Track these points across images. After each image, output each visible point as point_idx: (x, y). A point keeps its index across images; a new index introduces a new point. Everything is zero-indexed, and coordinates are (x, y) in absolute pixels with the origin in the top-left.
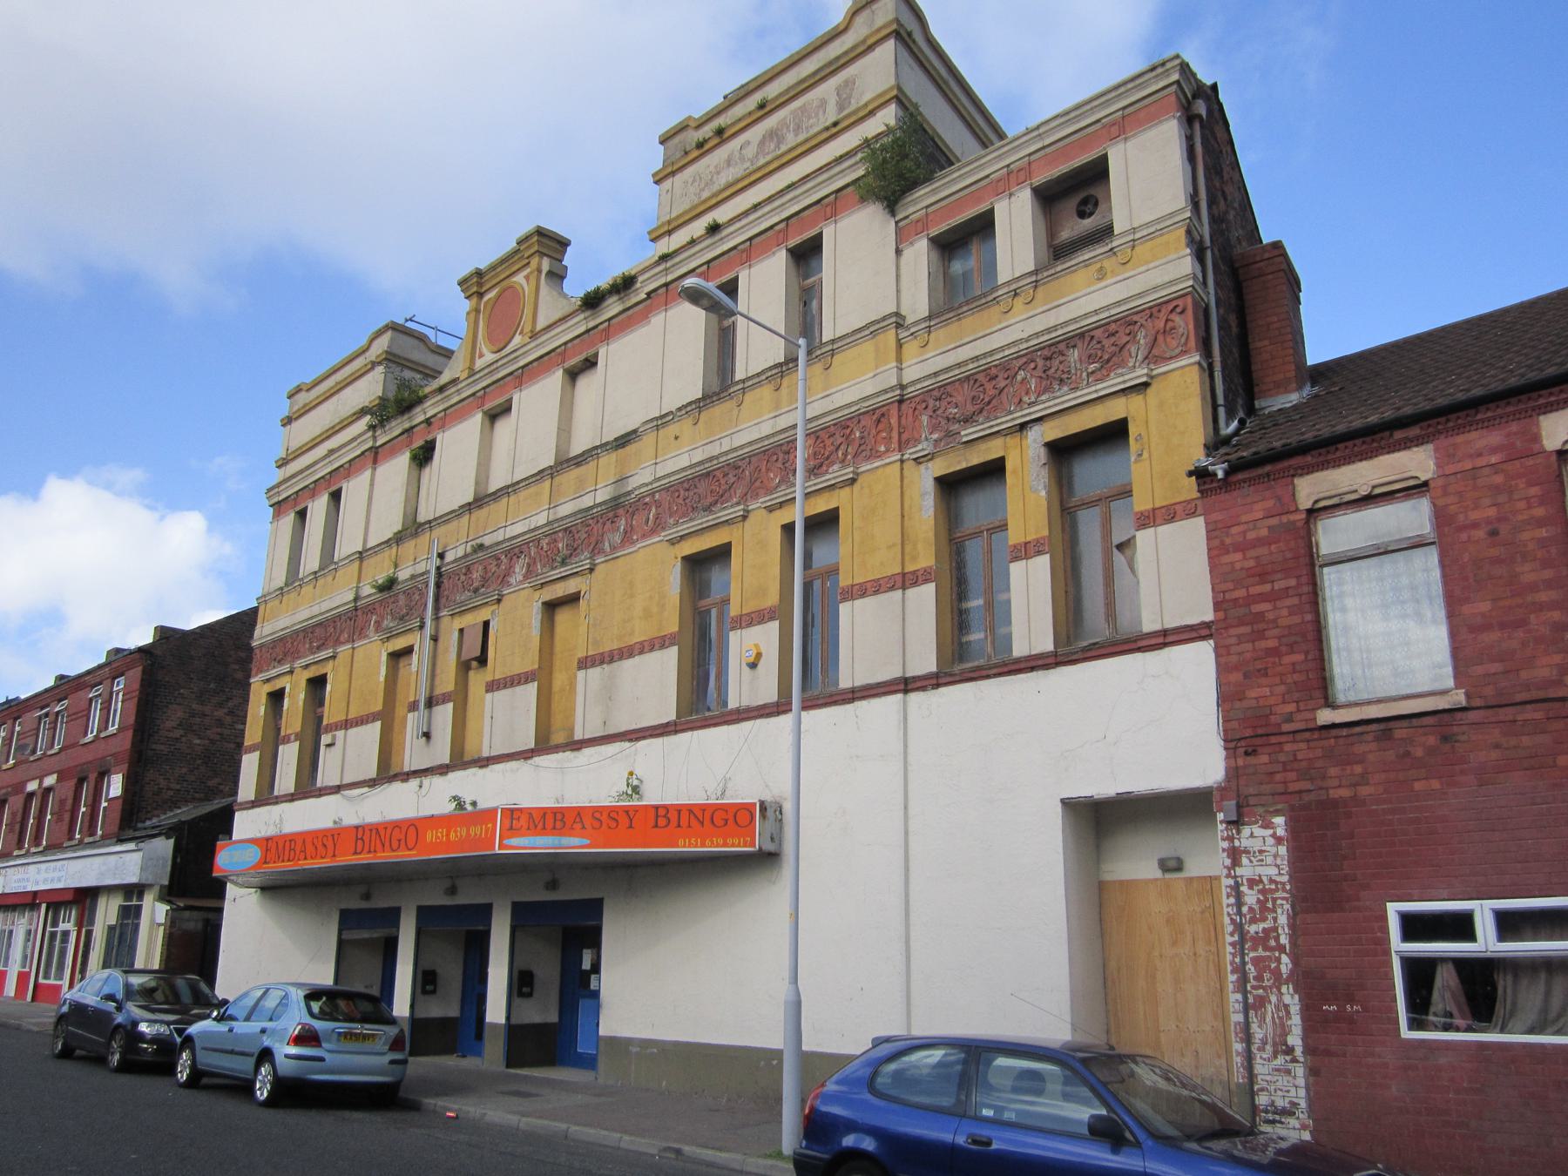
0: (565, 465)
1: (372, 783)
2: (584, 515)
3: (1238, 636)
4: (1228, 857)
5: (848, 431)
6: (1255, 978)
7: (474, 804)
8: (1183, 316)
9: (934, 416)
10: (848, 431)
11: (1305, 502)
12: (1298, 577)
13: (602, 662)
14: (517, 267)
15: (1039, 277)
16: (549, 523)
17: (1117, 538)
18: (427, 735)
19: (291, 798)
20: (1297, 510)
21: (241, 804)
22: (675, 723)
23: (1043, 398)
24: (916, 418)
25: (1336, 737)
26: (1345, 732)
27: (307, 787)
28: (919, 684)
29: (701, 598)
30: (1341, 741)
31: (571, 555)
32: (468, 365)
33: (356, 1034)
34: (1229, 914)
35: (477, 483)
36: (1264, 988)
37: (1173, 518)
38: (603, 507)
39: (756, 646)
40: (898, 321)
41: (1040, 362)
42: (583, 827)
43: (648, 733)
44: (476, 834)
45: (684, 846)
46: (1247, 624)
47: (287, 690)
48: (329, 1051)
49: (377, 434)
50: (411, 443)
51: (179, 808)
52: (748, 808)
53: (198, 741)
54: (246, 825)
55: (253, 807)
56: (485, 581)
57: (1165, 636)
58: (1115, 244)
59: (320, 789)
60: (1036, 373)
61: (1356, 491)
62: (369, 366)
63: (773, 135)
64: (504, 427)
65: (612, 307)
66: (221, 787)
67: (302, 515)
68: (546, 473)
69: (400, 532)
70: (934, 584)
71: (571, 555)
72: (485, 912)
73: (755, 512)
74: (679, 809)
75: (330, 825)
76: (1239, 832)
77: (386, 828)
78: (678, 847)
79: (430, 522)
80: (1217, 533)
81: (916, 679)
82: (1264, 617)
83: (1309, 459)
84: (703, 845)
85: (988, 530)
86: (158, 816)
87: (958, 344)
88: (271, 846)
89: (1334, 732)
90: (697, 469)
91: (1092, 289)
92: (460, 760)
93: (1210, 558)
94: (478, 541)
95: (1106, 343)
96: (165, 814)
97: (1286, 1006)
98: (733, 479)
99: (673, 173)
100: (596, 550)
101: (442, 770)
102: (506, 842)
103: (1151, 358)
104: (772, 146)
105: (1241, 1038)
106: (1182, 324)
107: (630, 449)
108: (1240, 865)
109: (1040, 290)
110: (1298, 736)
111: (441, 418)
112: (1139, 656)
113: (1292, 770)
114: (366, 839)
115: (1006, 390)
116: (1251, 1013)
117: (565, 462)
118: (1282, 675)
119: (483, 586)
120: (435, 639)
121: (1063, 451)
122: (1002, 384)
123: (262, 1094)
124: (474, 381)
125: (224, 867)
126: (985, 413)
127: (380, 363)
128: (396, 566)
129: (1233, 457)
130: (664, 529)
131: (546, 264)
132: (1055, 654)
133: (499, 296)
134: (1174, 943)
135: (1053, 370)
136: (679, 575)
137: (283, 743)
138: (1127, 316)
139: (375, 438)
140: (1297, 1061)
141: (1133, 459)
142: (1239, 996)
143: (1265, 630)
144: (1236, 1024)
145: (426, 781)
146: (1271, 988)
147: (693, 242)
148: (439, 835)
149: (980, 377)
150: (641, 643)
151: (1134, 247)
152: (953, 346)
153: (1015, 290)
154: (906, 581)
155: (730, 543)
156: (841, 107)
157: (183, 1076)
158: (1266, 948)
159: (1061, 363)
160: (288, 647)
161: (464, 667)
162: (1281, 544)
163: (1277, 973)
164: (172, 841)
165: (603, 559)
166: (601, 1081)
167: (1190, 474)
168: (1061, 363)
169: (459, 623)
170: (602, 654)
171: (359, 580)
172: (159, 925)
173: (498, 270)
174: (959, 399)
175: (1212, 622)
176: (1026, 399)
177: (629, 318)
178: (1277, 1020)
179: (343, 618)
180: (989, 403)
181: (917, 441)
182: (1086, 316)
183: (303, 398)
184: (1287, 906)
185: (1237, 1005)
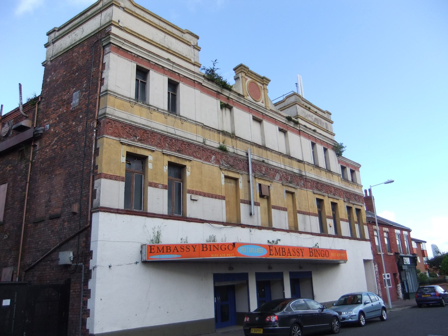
79: (240, 138)
147: (310, 129)
173: (253, 75)
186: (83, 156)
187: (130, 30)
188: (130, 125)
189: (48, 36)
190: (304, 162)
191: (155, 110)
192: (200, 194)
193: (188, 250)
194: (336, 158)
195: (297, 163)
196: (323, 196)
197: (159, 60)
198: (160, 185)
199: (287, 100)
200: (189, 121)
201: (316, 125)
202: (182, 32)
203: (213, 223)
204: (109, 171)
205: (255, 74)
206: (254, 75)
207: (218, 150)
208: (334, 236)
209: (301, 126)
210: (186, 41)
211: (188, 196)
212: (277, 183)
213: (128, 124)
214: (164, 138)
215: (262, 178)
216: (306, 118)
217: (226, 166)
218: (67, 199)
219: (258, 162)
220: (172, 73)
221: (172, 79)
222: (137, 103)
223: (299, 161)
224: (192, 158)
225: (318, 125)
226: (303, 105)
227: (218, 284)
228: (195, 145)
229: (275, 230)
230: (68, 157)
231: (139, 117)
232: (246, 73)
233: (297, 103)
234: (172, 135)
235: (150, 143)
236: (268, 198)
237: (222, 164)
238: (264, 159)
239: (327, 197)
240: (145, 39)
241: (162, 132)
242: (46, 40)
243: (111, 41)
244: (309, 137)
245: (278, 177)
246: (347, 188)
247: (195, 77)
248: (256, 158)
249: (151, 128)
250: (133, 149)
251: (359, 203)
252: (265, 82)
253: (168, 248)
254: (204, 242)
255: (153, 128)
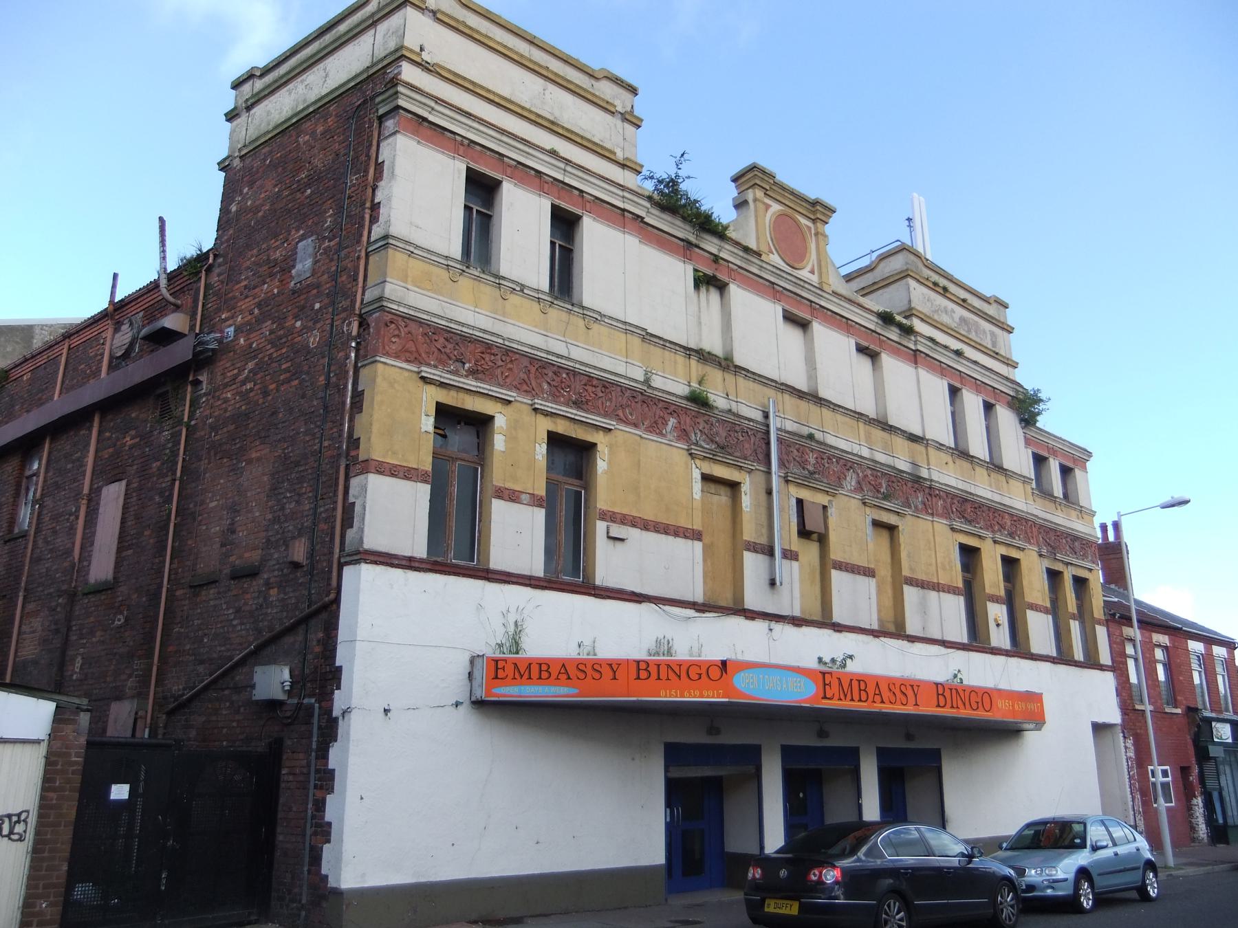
79: (748, 371)
147: (946, 347)
173: (786, 194)
186: (322, 411)
187: (450, 71)
188: (448, 331)
189: (234, 92)
190: (927, 440)
191: (514, 289)
192: (635, 522)
193: (597, 675)
194: (1020, 432)
195: (907, 443)
196: (980, 537)
197: (528, 153)
198: (523, 497)
199: (882, 264)
200: (606, 320)
201: (964, 336)
202: (591, 76)
203: (667, 603)
204: (390, 453)
205: (793, 193)
206: (789, 196)
207: (685, 402)
208: (1007, 653)
209: (919, 338)
210: (603, 100)
211: (601, 526)
212: (847, 498)
213: (442, 329)
214: (537, 366)
215: (806, 483)
216: (936, 317)
217: (706, 449)
218: (276, 527)
219: (797, 438)
220: (562, 188)
221: (563, 205)
222: (467, 270)
223: (913, 438)
224: (612, 423)
225: (970, 336)
227: (677, 773)
228: (623, 389)
229: (838, 628)
230: (281, 415)
231: (473, 309)
232: (767, 190)
233: (911, 274)
234: (559, 360)
235: (500, 379)
236: (822, 539)
237: (695, 441)
238: (813, 431)
239: (989, 542)
240: (491, 97)
241: (532, 352)
242: (229, 100)
243: (401, 102)
244: (941, 369)
245: (851, 481)
246: (1048, 517)
247: (625, 200)
248: (790, 426)
249: (503, 339)
250: (453, 397)
251: (1083, 560)
252: (819, 216)
253: (544, 667)
254: (642, 656)
255: (510, 340)
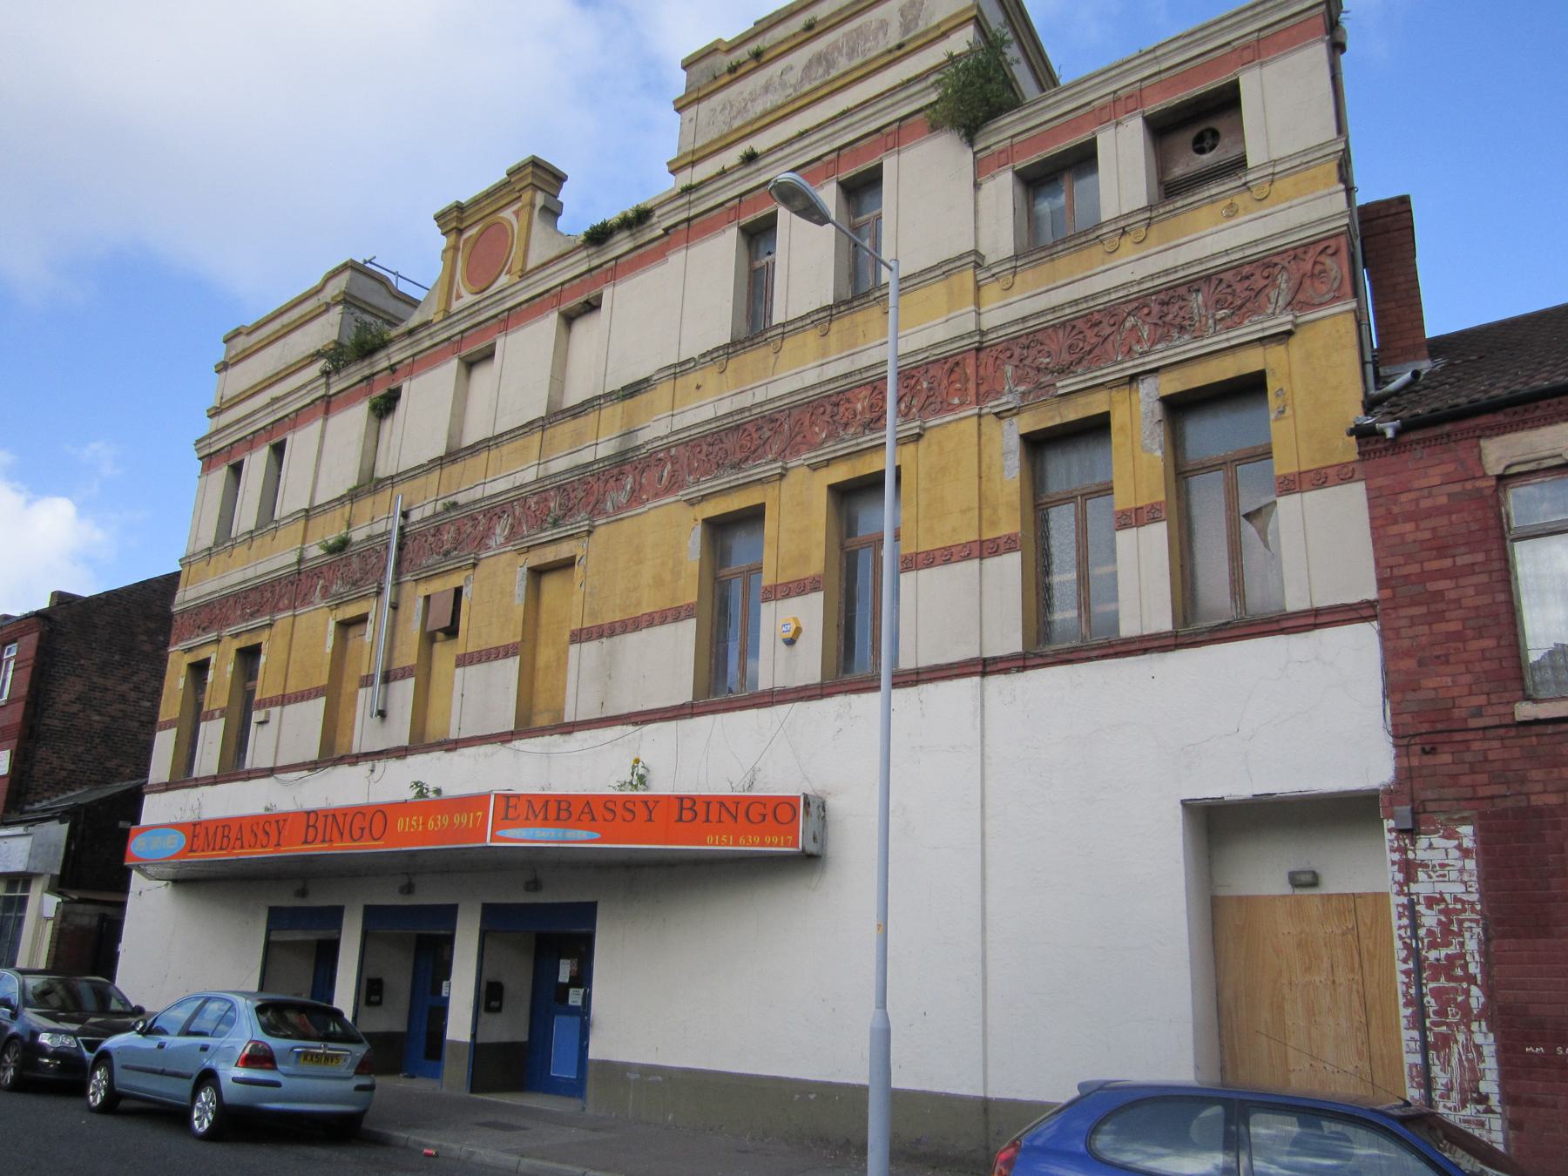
0: (560, 417)
1: (312, 766)
2: (582, 471)
3: (1412, 617)
4: (1400, 871)
5: (913, 382)
6: (1436, 1013)
7: (438, 791)
8: (1334, 258)
9: (1021, 365)
10: (913, 382)
11: (1494, 465)
12: (1487, 552)
13: (601, 636)
14: (504, 202)
15: (1154, 214)
16: (537, 481)
17: (1247, 506)
18: (382, 714)
19: (214, 781)
20: (1485, 476)
21: (152, 786)
22: (692, 705)
23: (1159, 347)
24: (997, 368)
25: (1537, 735)
26: (1550, 729)
27: (233, 768)
28: (1001, 666)
29: (722, 566)
30: (1546, 739)
31: (565, 515)
32: (442, 307)
33: (313, 1054)
34: (1400, 937)
35: (450, 436)
36: (1448, 1025)
37: (1324, 483)
38: (606, 463)
39: (795, 619)
40: (976, 260)
41: (1156, 308)
42: (593, 819)
43: (658, 716)
44: (461, 824)
45: (714, 844)
46: (1421, 604)
47: (213, 661)
48: (286, 1075)
49: (332, 380)
50: (371, 391)
51: (73, 790)
52: (789, 803)
53: (97, 718)
54: (155, 809)
55: (167, 790)
56: (458, 544)
57: (1316, 616)
58: (1250, 178)
59: (249, 772)
60: (1149, 320)
61: (1560, 455)
62: (323, 308)
63: (821, 59)
64: (483, 377)
65: (621, 244)
66: (122, 769)
67: (237, 469)
68: (536, 425)
69: (355, 488)
70: (1019, 554)
71: (565, 515)
72: (448, 914)
73: (795, 470)
74: (708, 801)
75: (261, 811)
76: (1414, 843)
77: (345, 815)
78: (706, 844)
79: (392, 477)
80: (1381, 501)
81: (995, 660)
82: (1443, 596)
83: (1500, 418)
84: (736, 843)
85: (1082, 495)
86: (49, 798)
87: (1050, 287)
88: (196, 831)
89: (1537, 729)
90: (725, 421)
91: (1220, 227)
92: (420, 743)
93: (1374, 528)
94: (452, 499)
95: (1238, 287)
96: (57, 796)
97: (1478, 1047)
98: (768, 434)
99: (699, 100)
100: (596, 510)
101: (400, 753)
102: (499, 833)
103: (1296, 303)
104: (821, 71)
105: (1418, 1083)
106: (1335, 267)
107: (641, 399)
108: (1416, 881)
109: (1154, 228)
110: (1491, 733)
111: (408, 365)
112: (1281, 638)
113: (1483, 772)
114: (320, 825)
115: (1111, 338)
116: (1432, 1054)
117: (556, 415)
118: (1467, 662)
119: (455, 549)
120: (395, 607)
121: (1178, 408)
122: (1108, 331)
123: (202, 1122)
124: (450, 324)
125: (137, 855)
126: (1085, 363)
127: (338, 303)
128: (349, 526)
129: (1405, 414)
130: (681, 487)
131: (540, 199)
132: (1174, 634)
133: (481, 234)
134: (1308, 969)
135: (1170, 316)
136: (699, 539)
137: (206, 719)
138: (1265, 257)
139: (328, 385)
140: (1493, 1112)
141: (1272, 416)
142: (1415, 1034)
143: (1444, 611)
144: (1411, 1066)
145: (380, 765)
146: (1457, 1024)
147: (723, 173)
148: (414, 823)
149: (1080, 324)
150: (650, 614)
151: (1272, 182)
152: (1044, 289)
153: (1123, 228)
154: (986, 549)
155: (763, 505)
156: (906, 28)
157: (96, 1098)
158: (1450, 978)
159: (1181, 308)
160: (213, 613)
161: (429, 638)
162: (1465, 514)
163: (1465, 1008)
164: (66, 827)
165: (604, 521)
166: (590, 1111)
167: (1351, 432)
168: (1181, 308)
169: (423, 589)
170: (600, 626)
171: (304, 542)
172: (48, 919)
174: (1053, 347)
175: (1377, 601)
176: (1137, 348)
177: (641, 256)
178: (1465, 1063)
179: (284, 582)
180: (1090, 352)
181: (999, 394)
182: (1214, 256)
183: (242, 343)
184: (1478, 930)
185: (1412, 1044)
219: (432, 520)
226: (715, 78)
